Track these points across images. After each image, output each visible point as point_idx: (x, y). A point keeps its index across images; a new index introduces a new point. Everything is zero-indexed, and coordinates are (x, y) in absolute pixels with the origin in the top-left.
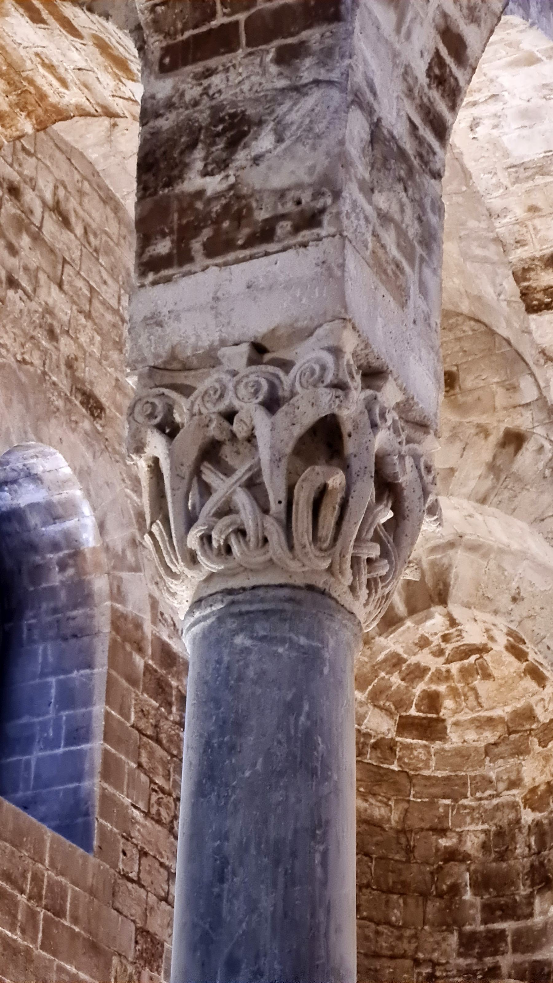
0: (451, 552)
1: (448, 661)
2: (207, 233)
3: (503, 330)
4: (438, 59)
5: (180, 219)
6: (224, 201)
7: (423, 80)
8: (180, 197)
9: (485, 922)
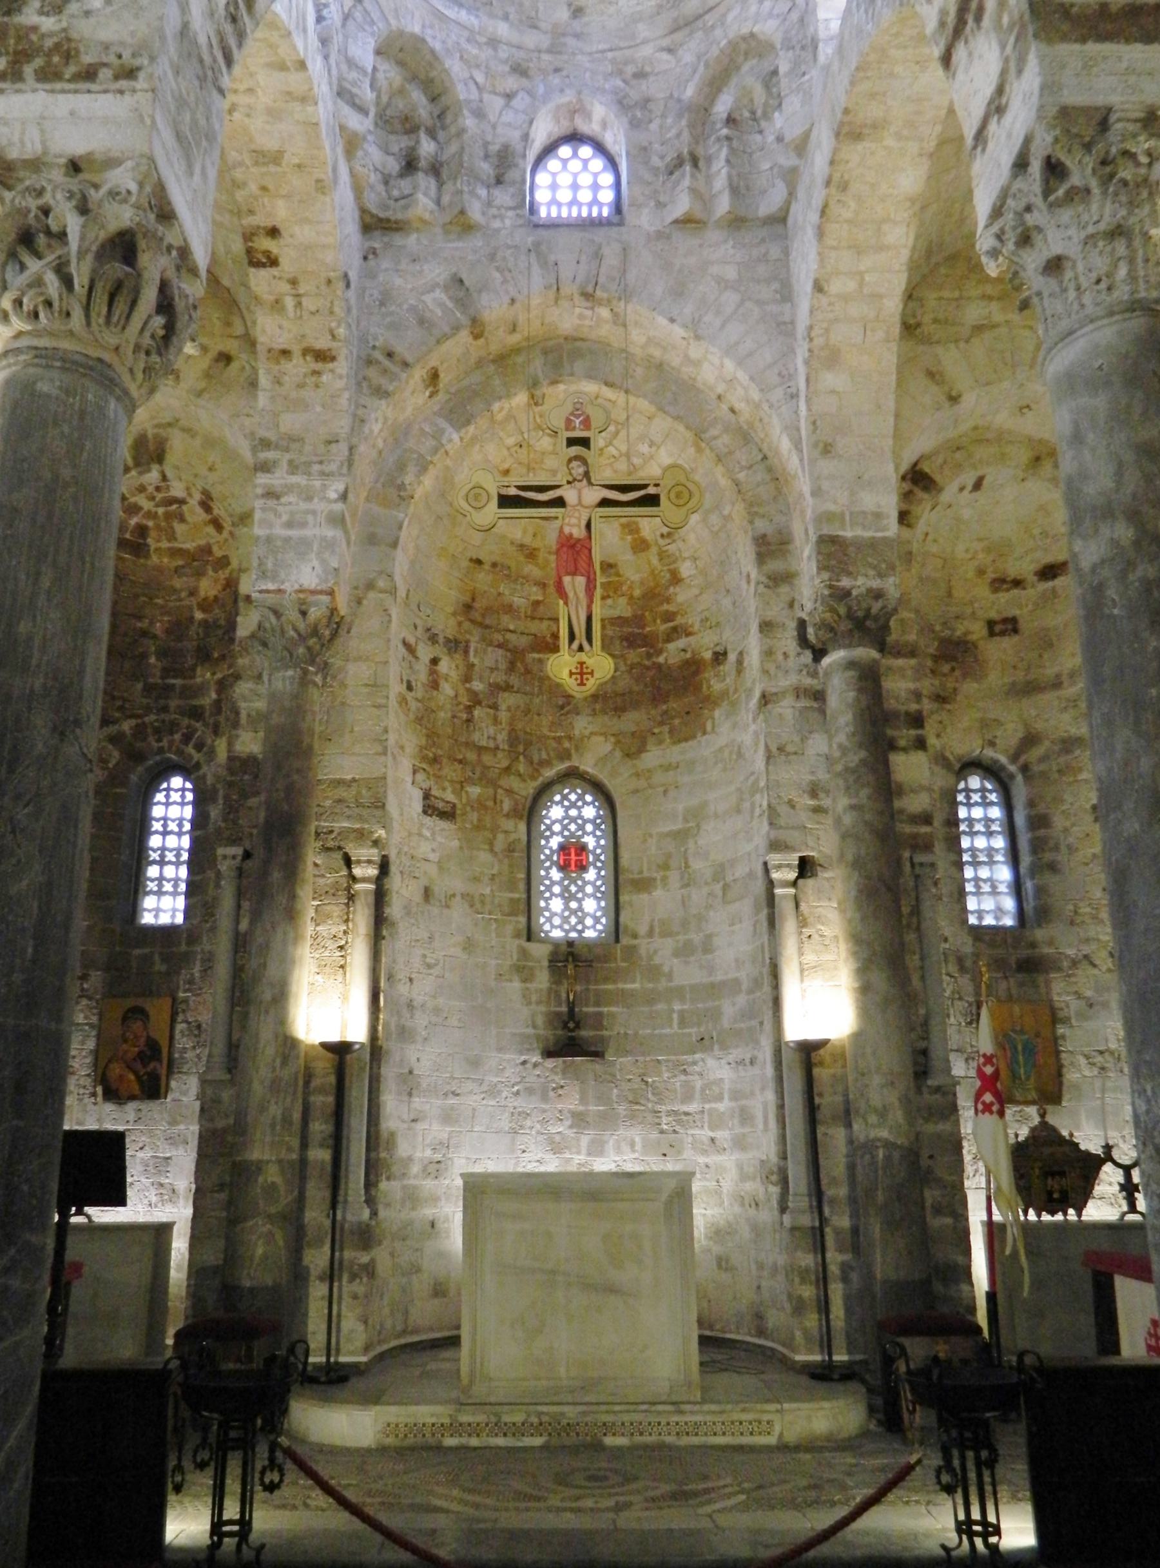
0: (169, 430)
1: (157, 506)
2: (39, 62)
3: (226, 282)
5: (17, 43)
6: (55, 39)
9: (162, 678)
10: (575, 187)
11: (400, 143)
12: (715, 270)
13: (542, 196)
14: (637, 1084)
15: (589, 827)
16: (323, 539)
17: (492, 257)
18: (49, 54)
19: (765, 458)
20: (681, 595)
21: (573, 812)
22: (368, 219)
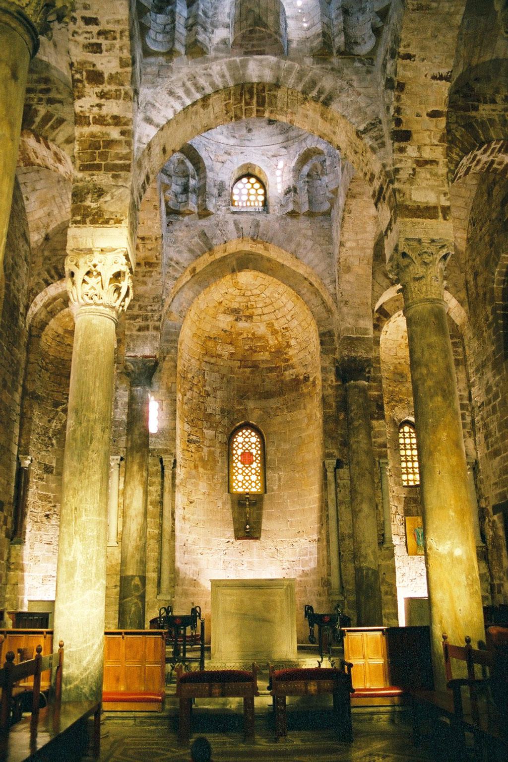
2: (91, 218)
4: (144, 183)
7: (140, 187)
8: (84, 206)
10: (249, 194)
11: (181, 181)
12: (303, 231)
13: (235, 198)
14: (273, 550)
15: (253, 446)
16: (153, 335)
17: (217, 225)
18: (94, 215)
19: (324, 303)
20: (291, 352)
21: (247, 440)
22: (169, 210)
